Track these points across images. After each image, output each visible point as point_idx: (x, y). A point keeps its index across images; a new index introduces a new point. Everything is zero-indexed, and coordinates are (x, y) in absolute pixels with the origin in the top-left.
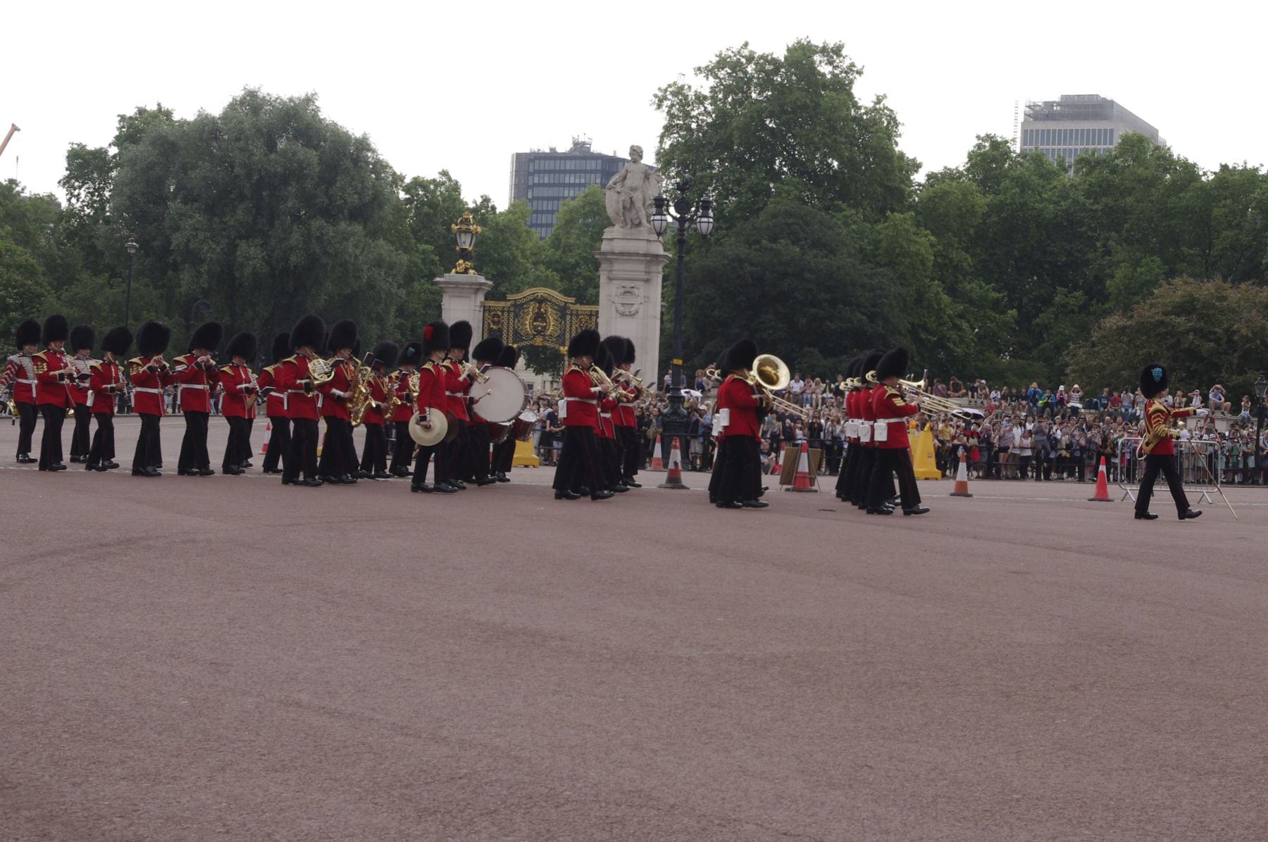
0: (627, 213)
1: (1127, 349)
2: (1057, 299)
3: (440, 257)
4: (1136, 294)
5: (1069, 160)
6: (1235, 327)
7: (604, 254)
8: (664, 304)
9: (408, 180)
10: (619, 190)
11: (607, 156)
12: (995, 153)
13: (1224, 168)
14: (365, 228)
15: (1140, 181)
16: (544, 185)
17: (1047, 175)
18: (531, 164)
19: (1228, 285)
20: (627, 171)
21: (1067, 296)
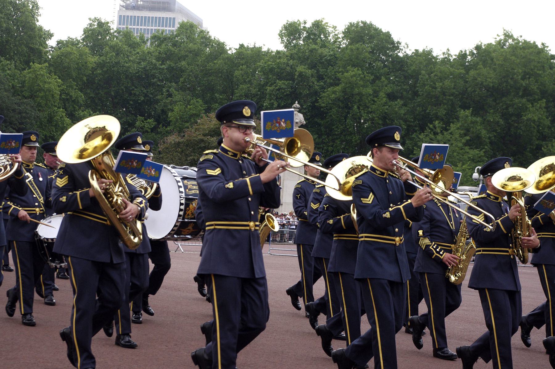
1: (181, 156)
2: (138, 124)
4: (187, 122)
5: (148, 36)
12: (101, 30)
13: (242, 46)
15: (190, 52)
17: (134, 45)
21: (143, 122)
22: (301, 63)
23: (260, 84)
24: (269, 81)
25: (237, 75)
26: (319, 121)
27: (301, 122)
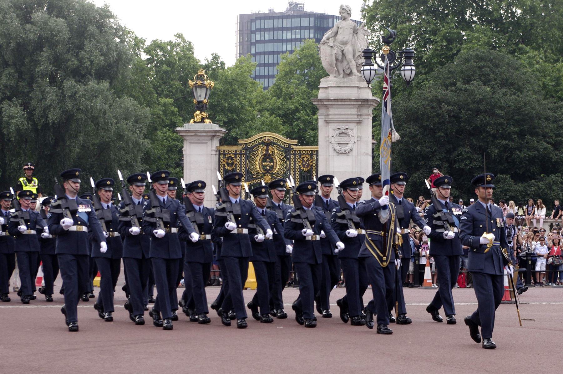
0: (339, 64)
3: (179, 108)
7: (321, 100)
8: (374, 141)
9: (148, 43)
10: (332, 44)
11: (318, 14)
14: (111, 84)
16: (264, 42)
18: (253, 24)
20: (338, 28)
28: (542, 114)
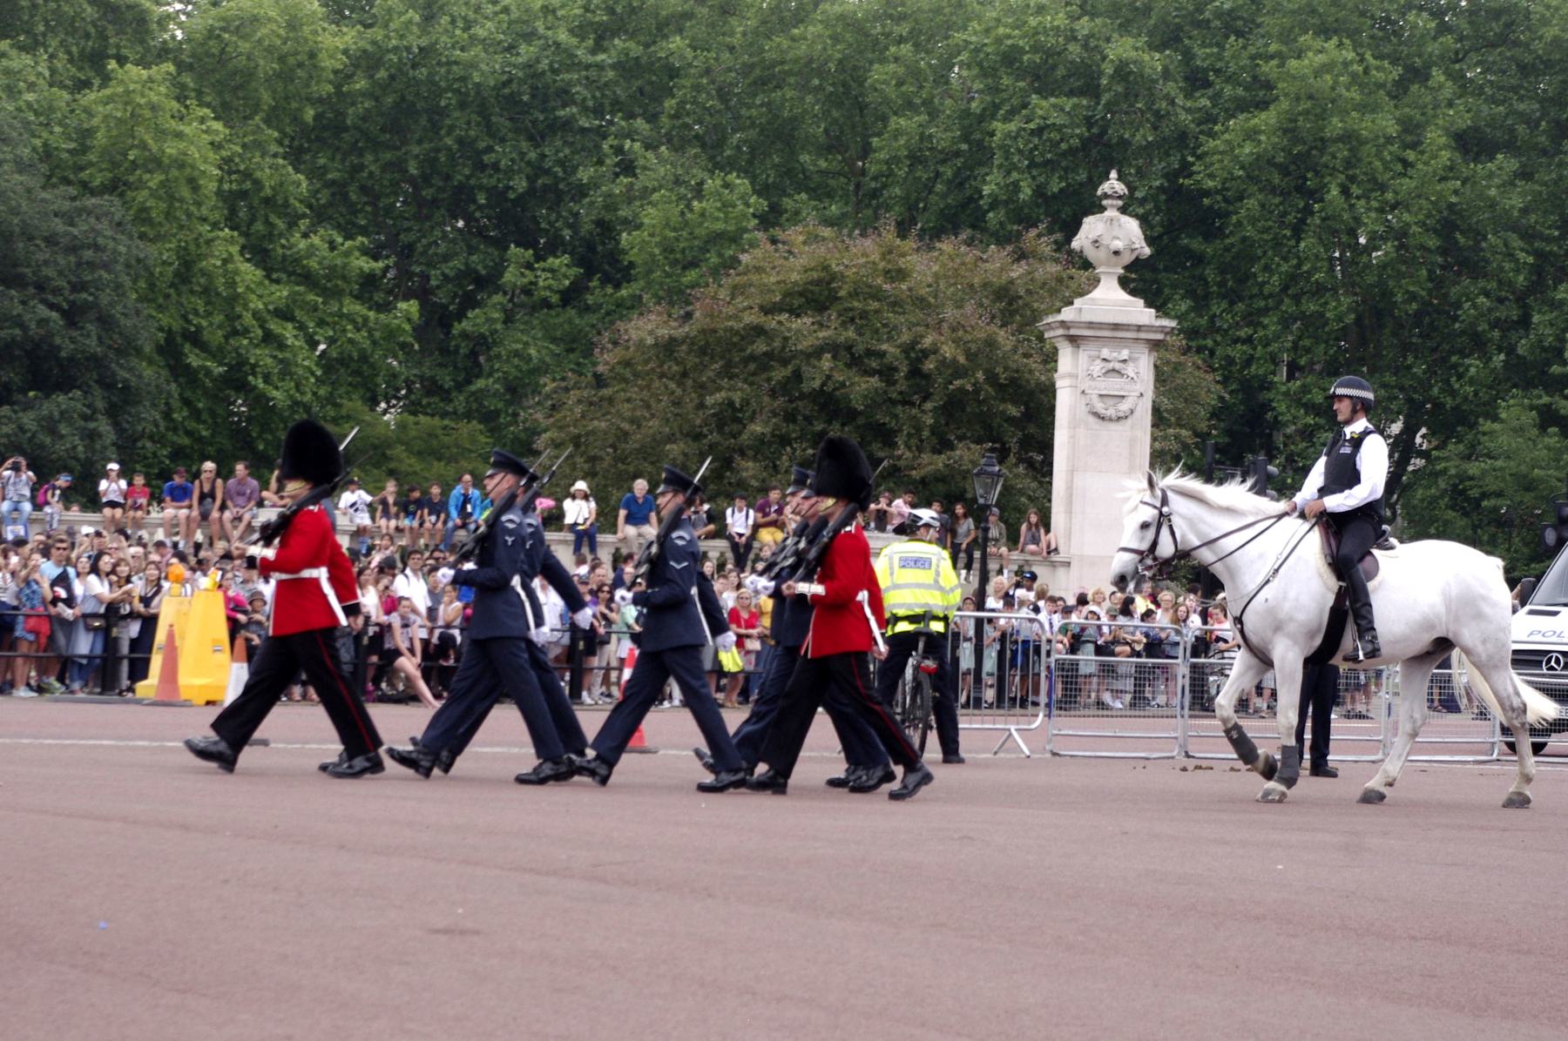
1: (679, 392)
2: (510, 276)
4: (693, 264)
6: (927, 341)
19: (910, 244)
21: (529, 266)
22: (1124, 28)
23: (966, 113)
24: (1003, 101)
25: (877, 80)
26: (1196, 244)
27: (1133, 250)
28: (37, 228)
